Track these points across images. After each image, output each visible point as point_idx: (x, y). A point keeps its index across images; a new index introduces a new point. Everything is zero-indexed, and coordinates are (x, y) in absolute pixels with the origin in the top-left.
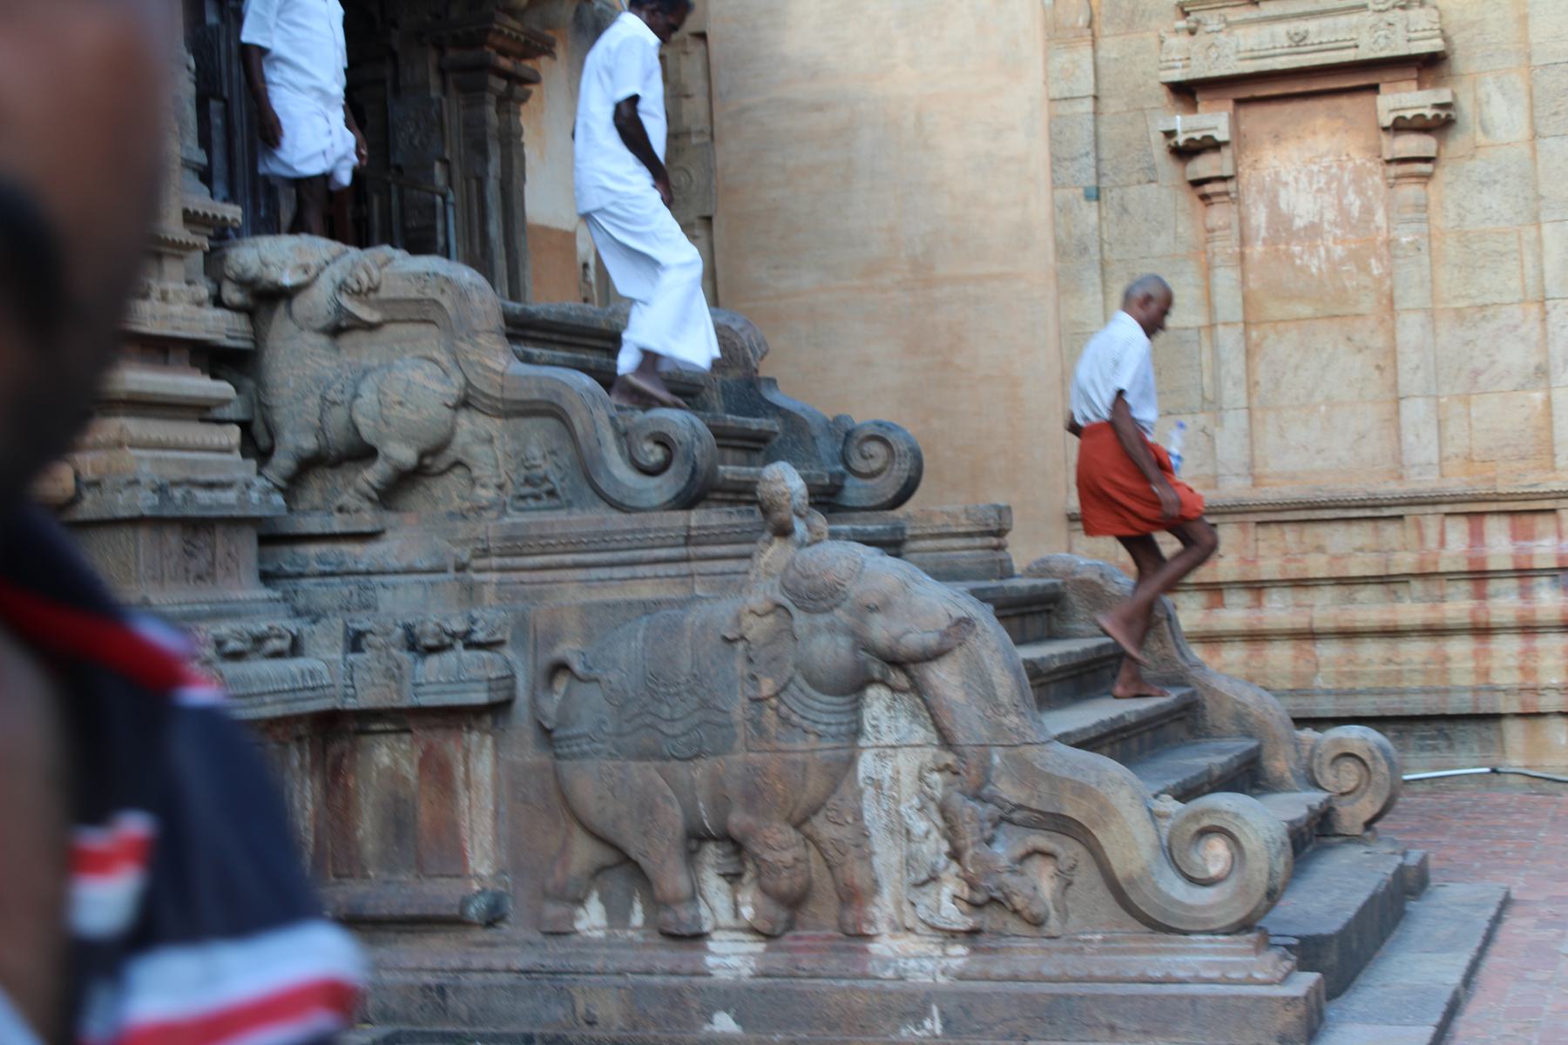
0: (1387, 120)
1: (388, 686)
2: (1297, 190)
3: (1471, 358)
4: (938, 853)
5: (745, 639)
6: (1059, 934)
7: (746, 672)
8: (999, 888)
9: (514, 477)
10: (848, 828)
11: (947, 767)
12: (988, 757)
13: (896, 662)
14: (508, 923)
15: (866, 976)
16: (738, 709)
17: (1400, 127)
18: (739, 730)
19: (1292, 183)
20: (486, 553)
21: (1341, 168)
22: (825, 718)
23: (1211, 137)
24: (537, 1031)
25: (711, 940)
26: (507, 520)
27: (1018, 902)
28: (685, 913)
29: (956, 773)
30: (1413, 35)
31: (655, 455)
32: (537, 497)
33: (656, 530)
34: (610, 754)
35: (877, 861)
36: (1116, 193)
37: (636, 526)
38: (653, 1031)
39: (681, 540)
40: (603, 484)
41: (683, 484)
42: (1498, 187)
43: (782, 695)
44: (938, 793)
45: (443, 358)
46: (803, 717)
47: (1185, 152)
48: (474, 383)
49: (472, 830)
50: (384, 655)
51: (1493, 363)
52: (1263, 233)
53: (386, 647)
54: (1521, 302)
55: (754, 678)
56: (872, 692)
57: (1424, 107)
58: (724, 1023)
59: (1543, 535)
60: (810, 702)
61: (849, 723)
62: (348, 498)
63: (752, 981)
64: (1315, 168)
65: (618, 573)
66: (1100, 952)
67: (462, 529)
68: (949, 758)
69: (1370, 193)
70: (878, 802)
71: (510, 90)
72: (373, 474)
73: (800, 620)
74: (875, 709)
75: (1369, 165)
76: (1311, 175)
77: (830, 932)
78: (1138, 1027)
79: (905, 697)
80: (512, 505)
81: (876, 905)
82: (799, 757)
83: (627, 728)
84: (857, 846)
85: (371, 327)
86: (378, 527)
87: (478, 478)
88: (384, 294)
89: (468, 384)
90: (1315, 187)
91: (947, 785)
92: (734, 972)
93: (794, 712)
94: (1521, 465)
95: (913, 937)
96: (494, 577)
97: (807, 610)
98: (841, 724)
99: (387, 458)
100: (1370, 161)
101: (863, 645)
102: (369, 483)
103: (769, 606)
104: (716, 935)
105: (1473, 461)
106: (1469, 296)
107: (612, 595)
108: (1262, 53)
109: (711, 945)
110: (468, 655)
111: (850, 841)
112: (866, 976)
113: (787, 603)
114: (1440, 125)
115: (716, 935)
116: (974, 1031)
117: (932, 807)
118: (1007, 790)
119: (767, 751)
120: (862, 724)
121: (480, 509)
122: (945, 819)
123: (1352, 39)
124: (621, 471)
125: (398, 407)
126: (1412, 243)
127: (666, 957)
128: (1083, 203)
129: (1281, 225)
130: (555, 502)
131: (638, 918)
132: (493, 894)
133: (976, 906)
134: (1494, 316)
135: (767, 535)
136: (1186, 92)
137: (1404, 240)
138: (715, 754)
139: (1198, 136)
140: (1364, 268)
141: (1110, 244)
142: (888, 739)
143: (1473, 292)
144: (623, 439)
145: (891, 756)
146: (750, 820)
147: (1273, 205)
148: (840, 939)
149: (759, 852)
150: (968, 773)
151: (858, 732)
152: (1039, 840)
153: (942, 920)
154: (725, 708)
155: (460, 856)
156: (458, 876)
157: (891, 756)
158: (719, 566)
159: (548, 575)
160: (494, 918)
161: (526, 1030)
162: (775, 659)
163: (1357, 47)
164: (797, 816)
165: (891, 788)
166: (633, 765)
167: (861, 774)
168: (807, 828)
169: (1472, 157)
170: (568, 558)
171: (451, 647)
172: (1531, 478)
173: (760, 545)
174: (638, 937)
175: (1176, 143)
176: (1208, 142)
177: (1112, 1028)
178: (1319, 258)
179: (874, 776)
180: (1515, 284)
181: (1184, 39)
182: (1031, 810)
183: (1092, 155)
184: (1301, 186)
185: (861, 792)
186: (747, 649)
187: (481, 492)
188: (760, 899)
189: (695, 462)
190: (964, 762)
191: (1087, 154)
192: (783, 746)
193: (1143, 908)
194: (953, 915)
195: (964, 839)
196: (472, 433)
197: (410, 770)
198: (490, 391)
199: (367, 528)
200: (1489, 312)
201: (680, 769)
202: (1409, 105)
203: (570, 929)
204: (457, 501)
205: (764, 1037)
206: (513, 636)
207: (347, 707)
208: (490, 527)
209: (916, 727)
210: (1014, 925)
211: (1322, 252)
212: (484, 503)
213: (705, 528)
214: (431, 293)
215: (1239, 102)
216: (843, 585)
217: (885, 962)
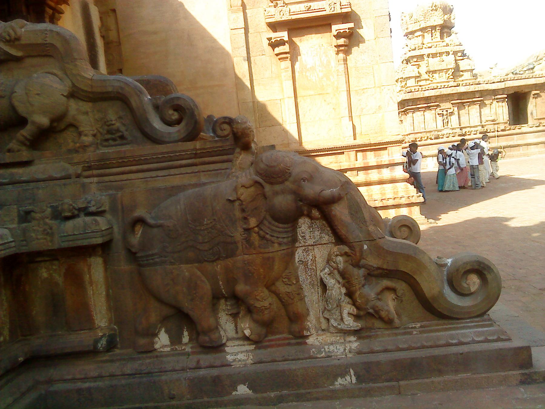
1: (45, 239)
4: (341, 293)
5: (240, 200)
8: (373, 308)
9: (101, 130)
10: (293, 286)
11: (346, 254)
14: (117, 348)
15: (311, 358)
16: (238, 235)
18: (240, 245)
20: (89, 168)
26: (98, 152)
27: (383, 314)
28: (214, 336)
30: (342, 7)
31: (175, 116)
32: (114, 140)
33: (180, 151)
37: (169, 150)
43: (260, 226)
44: (341, 266)
45: (59, 73)
48: (76, 84)
49: (95, 305)
50: (41, 222)
53: (43, 218)
58: (243, 390)
60: (274, 228)
61: (292, 236)
62: (13, 145)
63: (253, 367)
65: (160, 173)
66: (421, 332)
67: (77, 158)
68: (346, 249)
71: (53, 14)
72: (26, 132)
73: (268, 188)
77: (285, 335)
81: (309, 321)
84: (299, 294)
85: (18, 60)
86: (31, 159)
87: (83, 131)
88: (23, 42)
89: (73, 85)
91: (346, 262)
93: (267, 234)
96: (96, 179)
97: (271, 183)
98: (288, 237)
99: (33, 123)
101: (299, 197)
102: (23, 136)
103: (251, 182)
104: (229, 344)
105: (362, 135)
107: (160, 183)
109: (227, 349)
110: (88, 219)
111: (295, 293)
113: (261, 181)
115: (229, 344)
117: (336, 272)
118: (373, 261)
120: (297, 236)
121: (84, 147)
122: (344, 278)
123: (324, 8)
124: (157, 124)
125: (37, 97)
127: (206, 359)
128: (243, 62)
130: (125, 141)
131: (186, 338)
132: (109, 336)
135: (238, 150)
138: (227, 257)
139: (279, 39)
142: (310, 242)
145: (311, 250)
146: (248, 288)
148: (291, 339)
149: (253, 303)
150: (355, 255)
151: (295, 240)
152: (386, 283)
153: (346, 326)
154: (233, 235)
155: (90, 319)
156: (90, 329)
157: (311, 250)
158: (212, 167)
159: (125, 177)
160: (111, 345)
162: (256, 208)
165: (312, 265)
166: (183, 266)
167: (297, 260)
168: (273, 288)
170: (134, 168)
171: (78, 216)
173: (236, 155)
174: (188, 349)
176: (282, 41)
179: (302, 260)
181: (273, 8)
182: (383, 269)
185: (298, 268)
186: (241, 205)
191: (243, 46)
192: (262, 250)
193: (439, 310)
194: (350, 323)
195: (355, 286)
196: (77, 109)
197: (59, 279)
198: (86, 89)
199: (25, 159)
201: (209, 267)
203: (154, 349)
204: (71, 144)
207: (22, 251)
208: (91, 155)
209: (323, 235)
210: (378, 324)
212: (87, 144)
213: (204, 149)
214: (49, 40)
216: (289, 170)
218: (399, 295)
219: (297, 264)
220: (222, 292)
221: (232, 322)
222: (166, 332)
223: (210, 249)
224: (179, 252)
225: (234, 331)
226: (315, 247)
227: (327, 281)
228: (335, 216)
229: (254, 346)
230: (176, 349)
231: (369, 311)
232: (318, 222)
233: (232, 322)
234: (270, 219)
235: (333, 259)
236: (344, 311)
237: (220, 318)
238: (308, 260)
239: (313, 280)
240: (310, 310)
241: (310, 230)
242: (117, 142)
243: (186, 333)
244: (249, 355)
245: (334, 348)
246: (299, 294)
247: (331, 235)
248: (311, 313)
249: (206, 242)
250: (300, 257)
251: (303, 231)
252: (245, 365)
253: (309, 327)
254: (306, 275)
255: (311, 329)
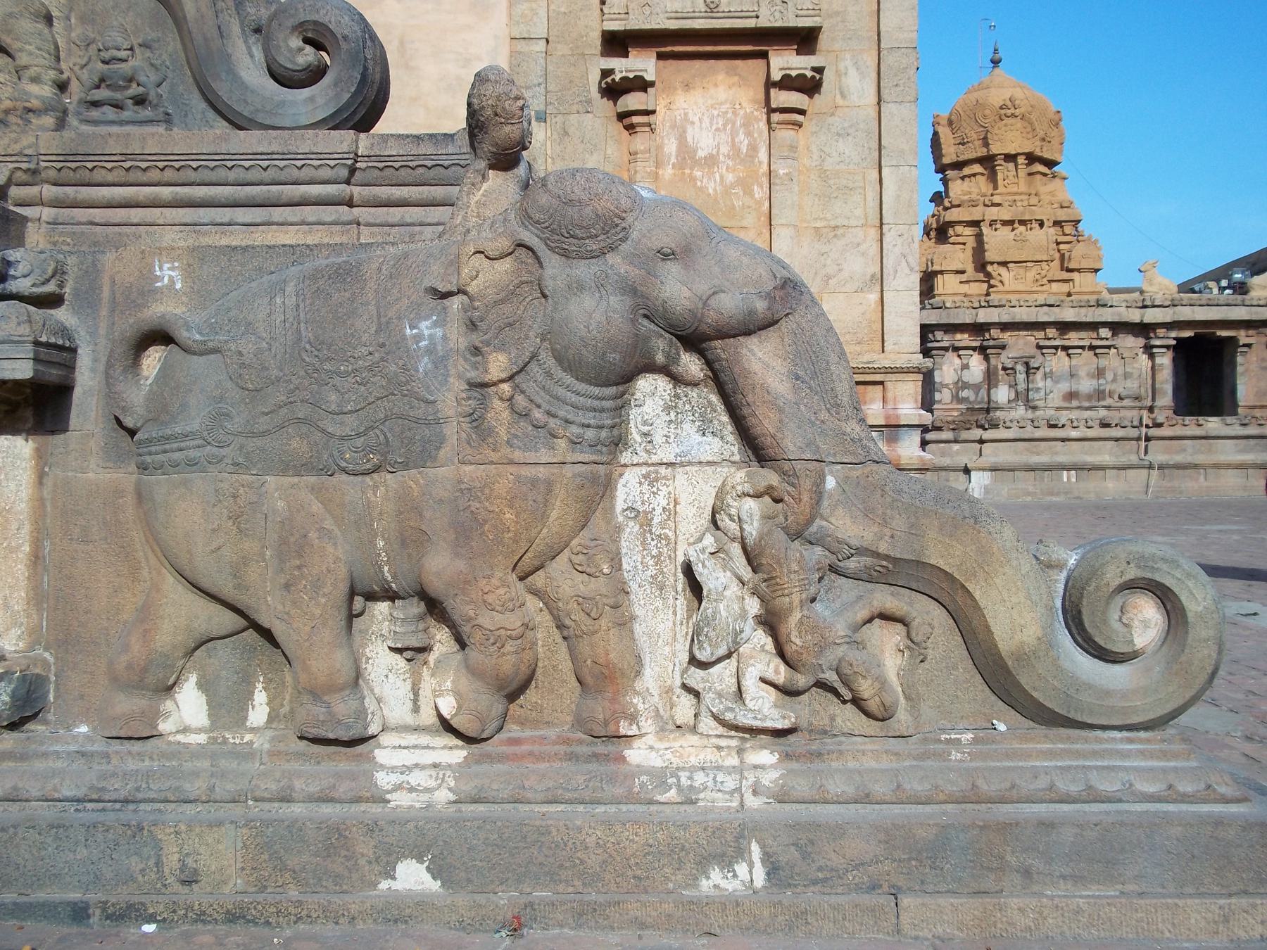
0: (776, 76)
2: (701, 128)
3: (825, 266)
4: (743, 615)
6: (911, 731)
7: (463, 343)
11: (769, 491)
12: (823, 480)
13: (694, 340)
17: (787, 83)
18: (450, 431)
19: (697, 123)
21: (735, 113)
22: (582, 417)
23: (641, 78)
24: (92, 897)
25: (379, 746)
27: (866, 688)
28: (343, 706)
29: (777, 501)
32: (118, 106)
34: (236, 464)
35: (638, 629)
36: (560, 119)
37: (275, 148)
38: (293, 893)
39: (344, 173)
40: (223, 89)
41: (346, 96)
42: (850, 138)
46: (549, 413)
47: (613, 90)
51: (840, 270)
52: (673, 160)
54: (862, 226)
55: (476, 351)
56: (645, 384)
57: (806, 69)
59: (872, 401)
64: (716, 113)
65: (242, 215)
68: (769, 477)
69: (756, 135)
70: (644, 544)
73: (555, 270)
74: (645, 408)
75: (755, 113)
76: (712, 118)
78: (1066, 871)
79: (693, 393)
80: (78, 114)
81: (638, 694)
82: (541, 472)
83: (263, 423)
84: (615, 607)
90: (714, 128)
91: (767, 518)
92: (425, 797)
94: (858, 348)
95: (694, 739)
96: (48, 213)
97: (566, 255)
100: (756, 110)
103: (504, 244)
104: (385, 739)
106: (826, 219)
108: (685, 15)
109: (381, 756)
112: (631, 799)
113: (534, 241)
114: (810, 85)
116: (815, 882)
117: (736, 549)
119: (492, 463)
126: (787, 174)
129: (687, 154)
130: (147, 113)
131: (258, 713)
133: (788, 692)
134: (843, 235)
136: (616, 43)
137: (781, 172)
138: (406, 466)
140: (748, 192)
141: (553, 159)
142: (666, 453)
143: (829, 216)
144: (252, 39)
147: (682, 139)
148: (580, 742)
151: (618, 442)
152: (885, 599)
157: (665, 478)
158: (396, 214)
159: (136, 214)
161: (75, 896)
163: (757, 17)
164: (527, 563)
165: (663, 525)
167: (620, 505)
168: (538, 579)
169: (833, 114)
170: (166, 192)
172: (866, 358)
174: (261, 742)
175: (613, 80)
177: (1027, 873)
178: (715, 182)
179: (638, 506)
180: (859, 212)
182: (877, 555)
183: (543, 85)
184: (704, 125)
185: (619, 529)
187: (34, 89)
188: (465, 683)
189: (365, 69)
190: (793, 485)
192: (517, 455)
193: (1035, 694)
200: (840, 232)
202: (794, 66)
205: (481, 899)
206: (76, 293)
211: (718, 178)
212: (35, 103)
215: (661, 56)
217: (661, 777)
218: (918, 639)
219: (620, 519)
220: (383, 572)
221: (402, 677)
222: (201, 685)
223: (359, 435)
224: (264, 434)
225: (410, 704)
226: (680, 470)
227: (705, 572)
228: (747, 374)
229: (464, 753)
230: (225, 740)
231: (822, 676)
232: (695, 395)
233: (402, 677)
234: (551, 363)
235: (728, 506)
236: (749, 669)
237: (368, 659)
238: (654, 509)
239: (662, 572)
240: (647, 660)
241: (668, 418)
242: (126, 115)
243: (260, 697)
244: (444, 775)
245: (706, 779)
246: (615, 607)
247: (731, 438)
248: (647, 672)
249: (351, 412)
250: (631, 497)
251: (646, 417)
252: (429, 806)
253: (636, 711)
254: (645, 552)
255: (643, 718)
